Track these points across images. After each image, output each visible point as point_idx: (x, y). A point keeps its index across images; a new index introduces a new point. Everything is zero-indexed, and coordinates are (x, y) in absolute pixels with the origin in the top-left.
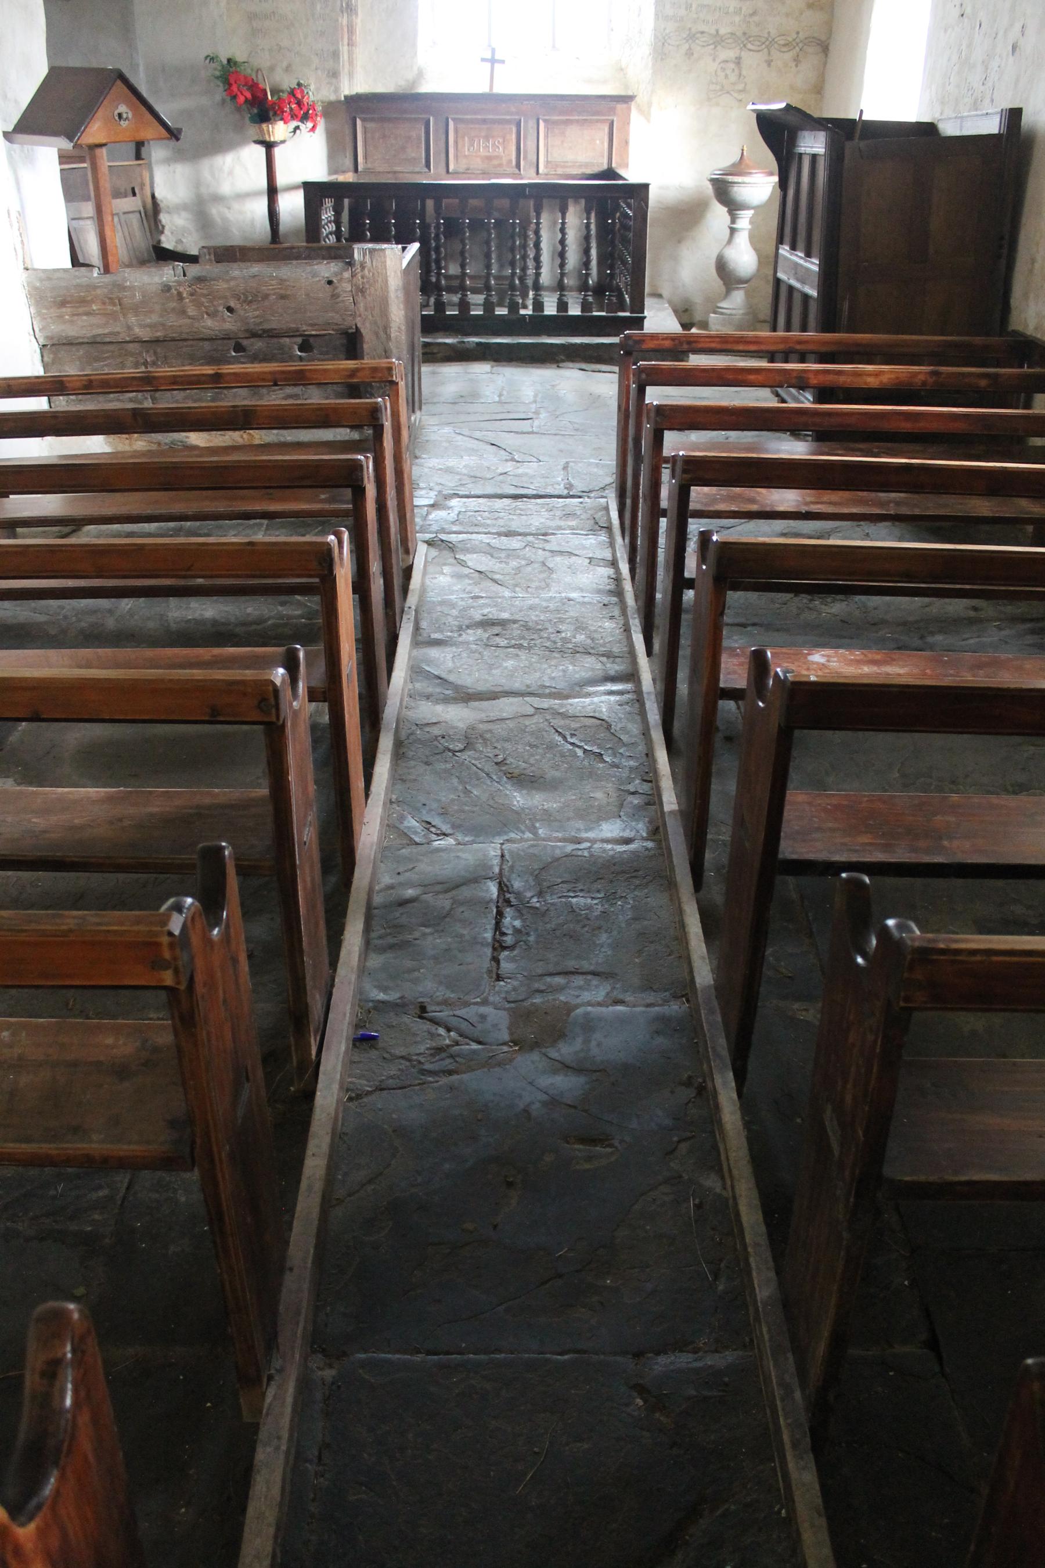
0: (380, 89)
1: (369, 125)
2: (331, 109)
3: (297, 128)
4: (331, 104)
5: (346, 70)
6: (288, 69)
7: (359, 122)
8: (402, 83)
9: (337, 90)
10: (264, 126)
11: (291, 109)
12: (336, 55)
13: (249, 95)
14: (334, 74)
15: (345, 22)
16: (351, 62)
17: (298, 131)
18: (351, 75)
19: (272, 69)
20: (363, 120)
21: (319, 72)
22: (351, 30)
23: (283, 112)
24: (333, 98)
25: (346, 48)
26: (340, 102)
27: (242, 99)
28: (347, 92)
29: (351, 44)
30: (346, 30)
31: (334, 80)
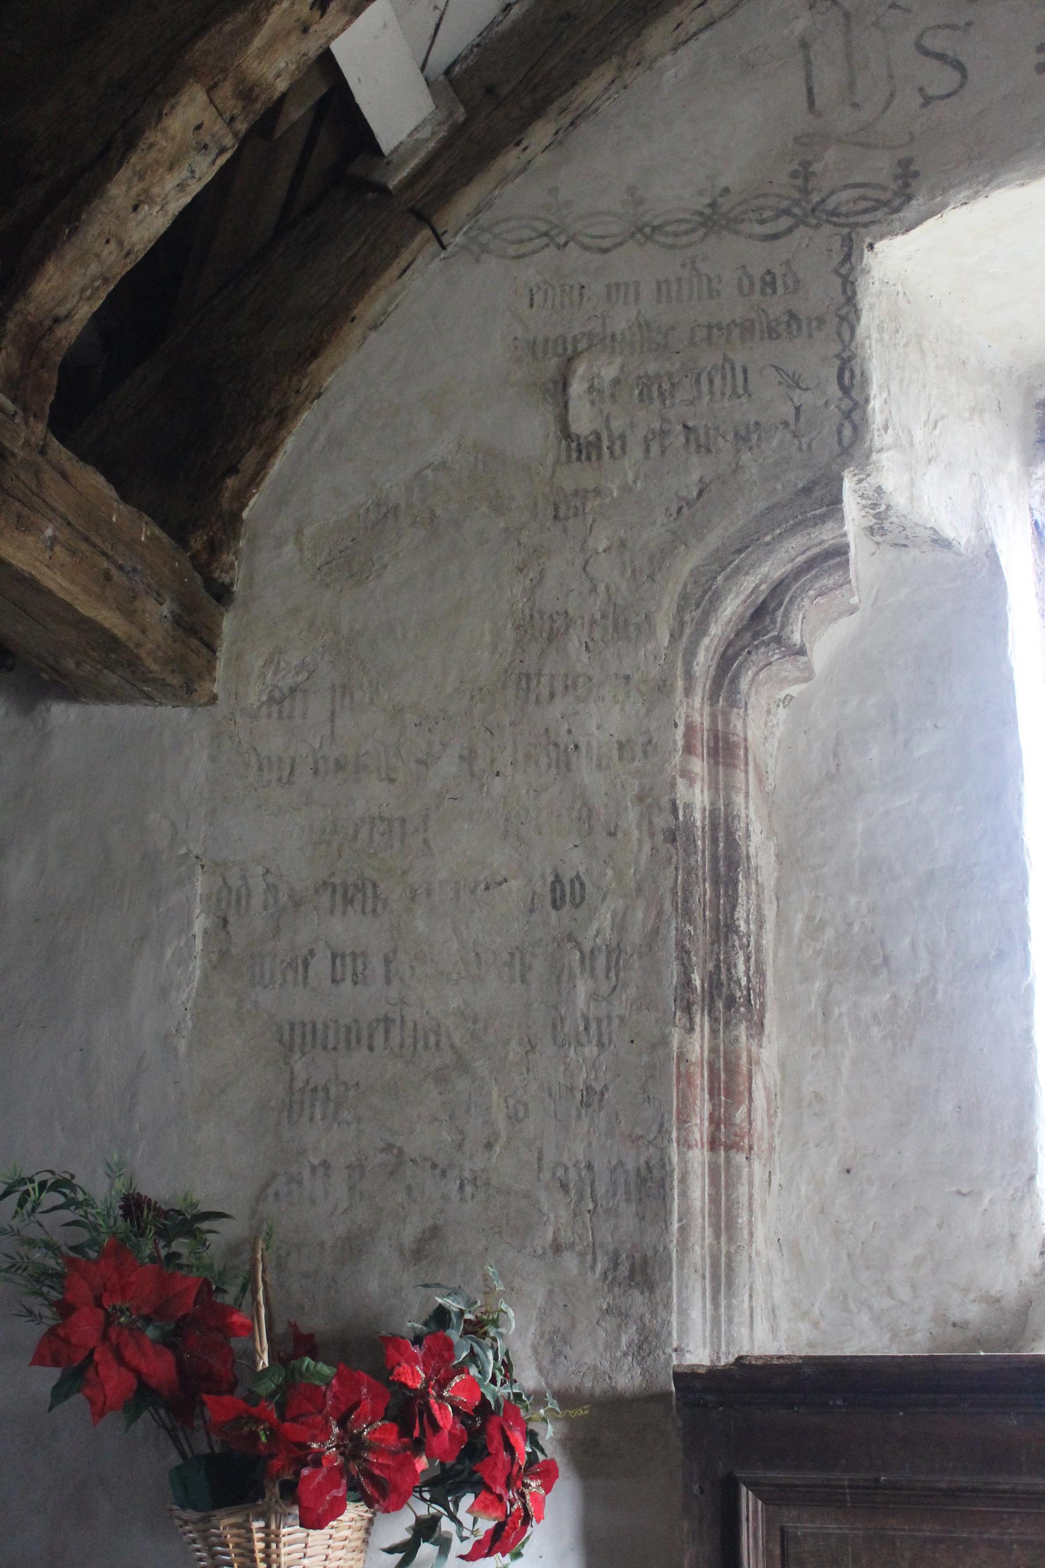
0: (864, 1339)
1: (806, 1525)
2: (606, 1433)
3: (426, 1529)
4: (613, 1405)
5: (699, 1252)
6: (425, 1248)
7: (749, 1502)
8: (973, 1312)
9: (649, 1342)
10: (225, 1525)
11: (353, 1447)
12: (651, 1186)
13: (161, 1368)
14: (641, 1273)
15: (698, 1047)
16: (724, 1219)
17: (427, 1550)
18: (722, 1278)
19: (354, 1247)
20: (774, 1497)
21: (570, 1262)
22: (727, 1081)
23: (302, 1456)
24: (628, 1379)
25: (699, 1157)
26: (662, 1397)
27: (115, 1380)
28: (699, 1355)
29: (725, 1139)
30: (701, 1081)
31: (638, 1299)
